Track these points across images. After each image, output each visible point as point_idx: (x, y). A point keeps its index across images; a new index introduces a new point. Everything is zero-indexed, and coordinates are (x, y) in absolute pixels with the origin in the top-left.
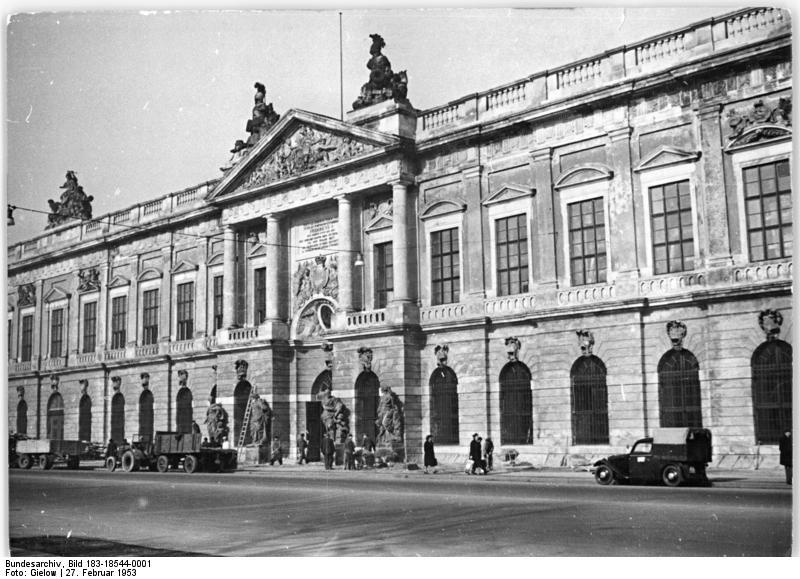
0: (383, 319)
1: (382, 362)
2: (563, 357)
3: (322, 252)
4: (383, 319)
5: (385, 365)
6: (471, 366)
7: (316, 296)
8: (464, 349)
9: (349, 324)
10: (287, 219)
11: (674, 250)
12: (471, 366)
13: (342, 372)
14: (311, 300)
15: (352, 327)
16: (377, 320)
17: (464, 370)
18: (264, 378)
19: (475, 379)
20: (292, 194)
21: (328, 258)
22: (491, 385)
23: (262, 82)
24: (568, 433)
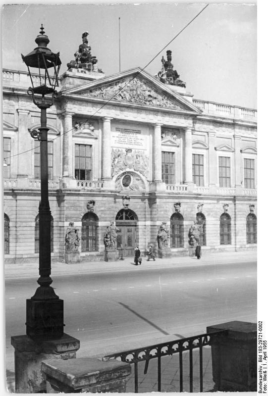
0: (186, 190)
1: (185, 209)
2: (244, 213)
3: (130, 147)
4: (186, 190)
5: (187, 211)
6: (212, 214)
7: (128, 170)
8: (209, 206)
9: (167, 189)
10: (114, 121)
11: (224, 179)
12: (212, 214)
13: (162, 212)
14: (124, 171)
15: (169, 191)
16: (170, 189)
17: (209, 215)
18: (108, 212)
19: (213, 219)
21: (133, 150)
22: (234, 223)
23: (81, 36)
24: (246, 240)
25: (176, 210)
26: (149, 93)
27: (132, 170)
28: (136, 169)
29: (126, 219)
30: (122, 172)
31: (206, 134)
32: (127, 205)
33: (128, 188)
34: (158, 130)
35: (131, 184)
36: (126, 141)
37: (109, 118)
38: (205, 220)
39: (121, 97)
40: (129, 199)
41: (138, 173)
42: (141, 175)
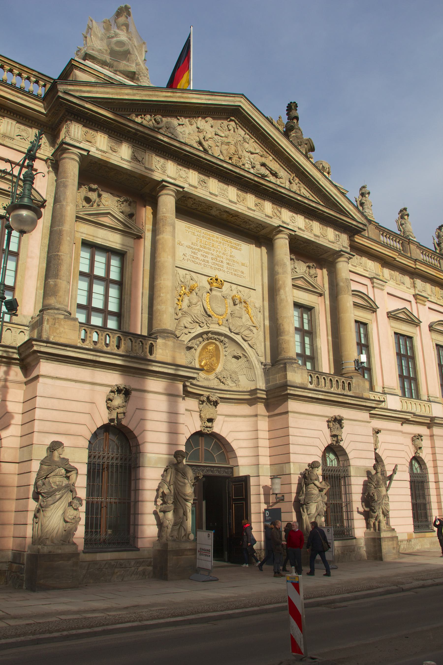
14: (205, 329)
25: (333, 436)
26: (263, 160)
27: (224, 330)
28: (233, 329)
29: (206, 460)
30: (199, 330)
31: (367, 282)
32: (210, 420)
33: (212, 376)
34: (282, 244)
35: (219, 368)
36: (210, 260)
37: (172, 187)
38: (383, 466)
40: (216, 404)
41: (238, 338)
42: (245, 345)
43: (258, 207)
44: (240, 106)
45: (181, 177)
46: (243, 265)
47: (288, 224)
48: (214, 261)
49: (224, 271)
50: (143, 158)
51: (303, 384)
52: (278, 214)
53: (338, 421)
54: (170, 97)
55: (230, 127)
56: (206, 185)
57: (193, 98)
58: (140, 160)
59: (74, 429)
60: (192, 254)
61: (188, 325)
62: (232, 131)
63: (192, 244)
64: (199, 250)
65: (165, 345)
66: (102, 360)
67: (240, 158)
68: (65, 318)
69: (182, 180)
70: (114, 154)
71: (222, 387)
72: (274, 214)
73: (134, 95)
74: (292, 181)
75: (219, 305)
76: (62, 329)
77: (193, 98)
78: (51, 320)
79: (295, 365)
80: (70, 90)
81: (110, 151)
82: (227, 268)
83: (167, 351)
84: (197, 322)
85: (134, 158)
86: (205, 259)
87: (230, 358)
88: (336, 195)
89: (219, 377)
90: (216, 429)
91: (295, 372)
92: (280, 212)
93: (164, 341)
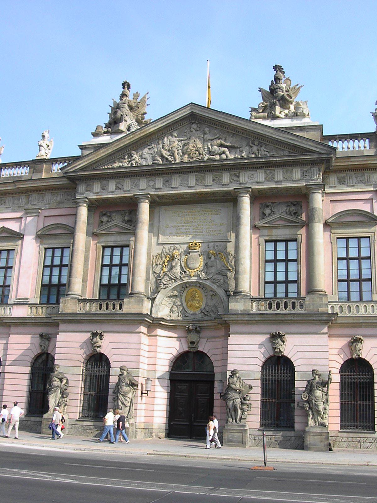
20: (176, 181)
32: (192, 343)
39: (165, 160)
43: (215, 181)
44: (192, 112)
45: (150, 186)
46: (221, 225)
47: (245, 184)
48: (195, 230)
49: (203, 235)
50: (123, 185)
51: (245, 310)
52: (236, 179)
53: (280, 336)
54: (133, 137)
55: (192, 129)
56: (169, 183)
57: (150, 129)
58: (120, 187)
59: (74, 357)
60: (177, 231)
61: (166, 282)
62: (194, 131)
63: (177, 223)
64: (183, 226)
65: (129, 302)
66: (85, 318)
67: (197, 151)
68: (71, 299)
69: (150, 188)
70: (105, 191)
71: (206, 318)
72: (232, 181)
73: (108, 150)
74: (252, 145)
75: (192, 262)
76: (69, 305)
77: (150, 129)
78: (64, 302)
79: (238, 297)
80: (69, 170)
81: (102, 190)
82: (207, 232)
83: (130, 306)
84: (173, 279)
85: (117, 188)
86: (187, 231)
87: (209, 297)
88: (292, 140)
89: (203, 311)
90: (200, 349)
91: (238, 302)
92: (239, 177)
93: (128, 300)
